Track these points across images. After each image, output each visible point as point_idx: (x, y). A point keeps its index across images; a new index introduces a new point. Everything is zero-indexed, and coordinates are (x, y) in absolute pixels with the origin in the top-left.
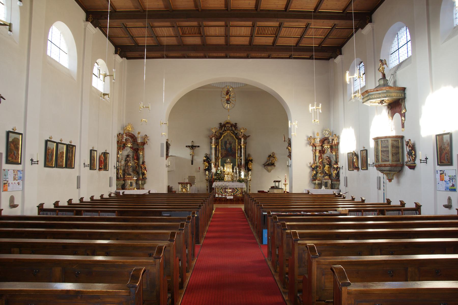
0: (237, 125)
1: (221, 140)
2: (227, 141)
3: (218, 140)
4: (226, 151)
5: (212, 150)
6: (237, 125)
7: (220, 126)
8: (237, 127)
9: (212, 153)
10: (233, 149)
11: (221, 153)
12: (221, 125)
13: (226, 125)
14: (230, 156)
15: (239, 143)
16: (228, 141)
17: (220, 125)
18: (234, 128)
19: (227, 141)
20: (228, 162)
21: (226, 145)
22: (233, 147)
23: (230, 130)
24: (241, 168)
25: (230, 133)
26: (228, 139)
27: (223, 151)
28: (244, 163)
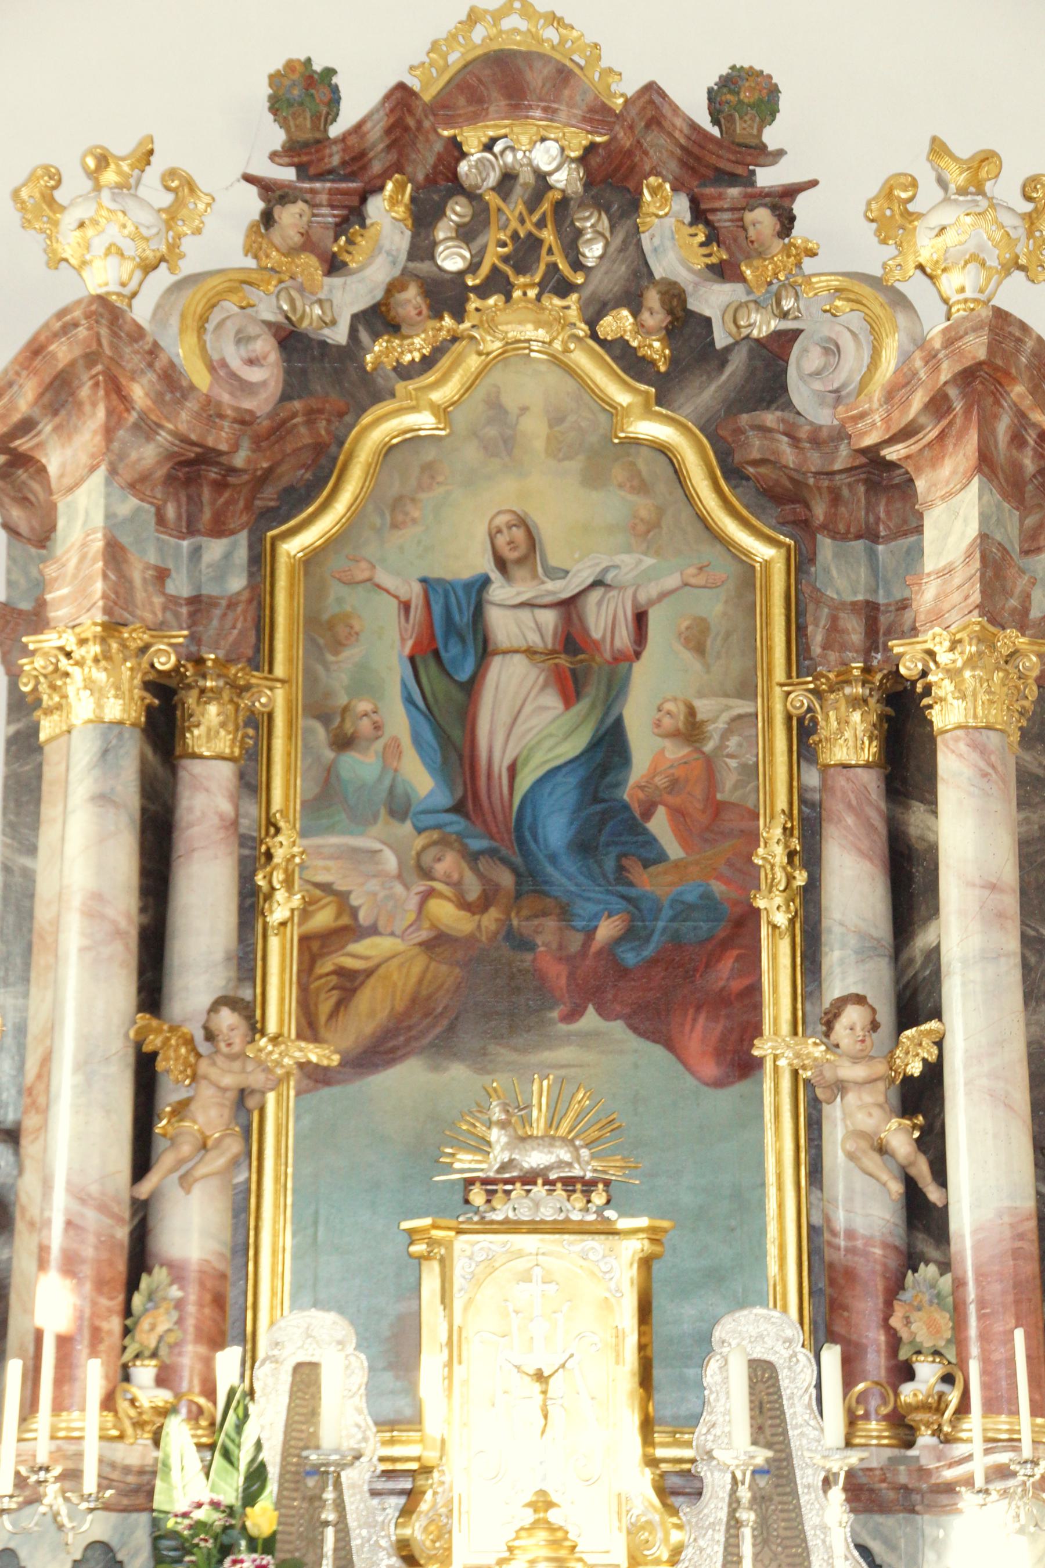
0: (772, 137)
1: (312, 559)
2: (485, 582)
3: (215, 549)
4: (448, 864)
5: (47, 836)
6: (772, 137)
7: (288, 174)
8: (791, 192)
9: (43, 914)
10: (659, 825)
11: (324, 918)
12: (322, 142)
13: (472, 138)
14: (591, 1019)
15: (854, 630)
16: (522, 589)
17: (277, 137)
18: (699, 214)
19: (485, 582)
20: (529, 1179)
21: (471, 688)
22: (675, 752)
23: (564, 289)
24: (928, 1372)
25: (570, 371)
26: (532, 540)
27: (390, 861)
28: (1029, 1204)
